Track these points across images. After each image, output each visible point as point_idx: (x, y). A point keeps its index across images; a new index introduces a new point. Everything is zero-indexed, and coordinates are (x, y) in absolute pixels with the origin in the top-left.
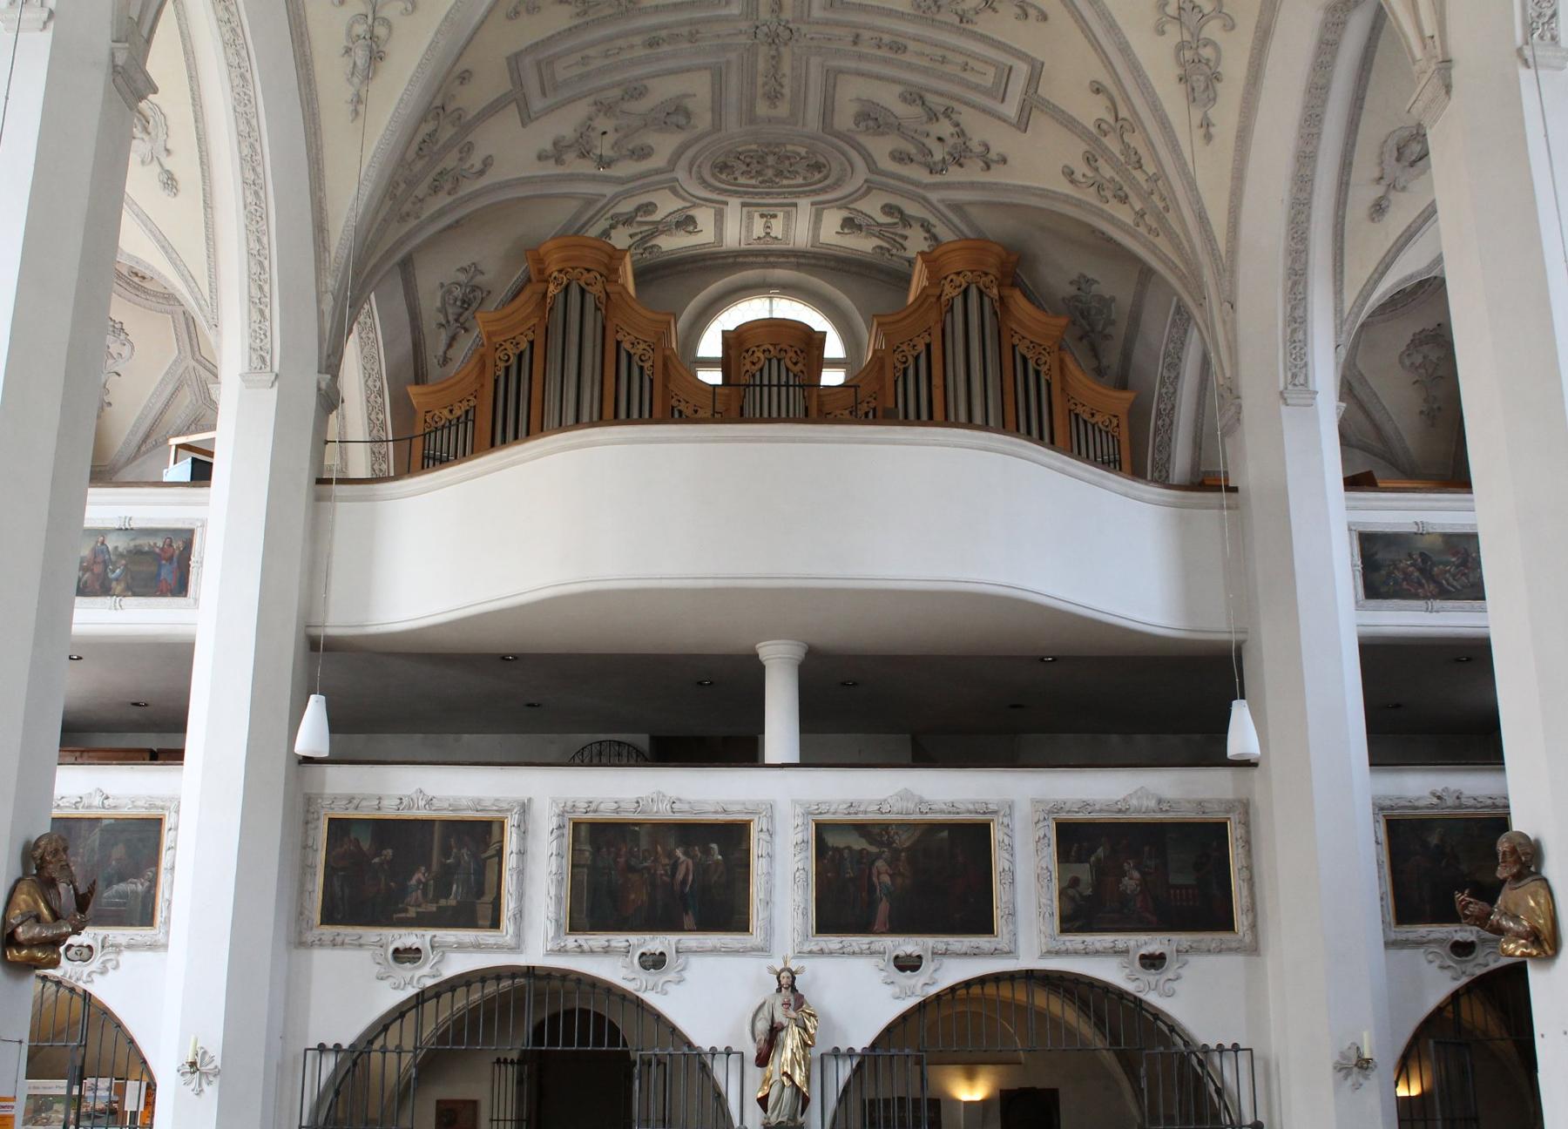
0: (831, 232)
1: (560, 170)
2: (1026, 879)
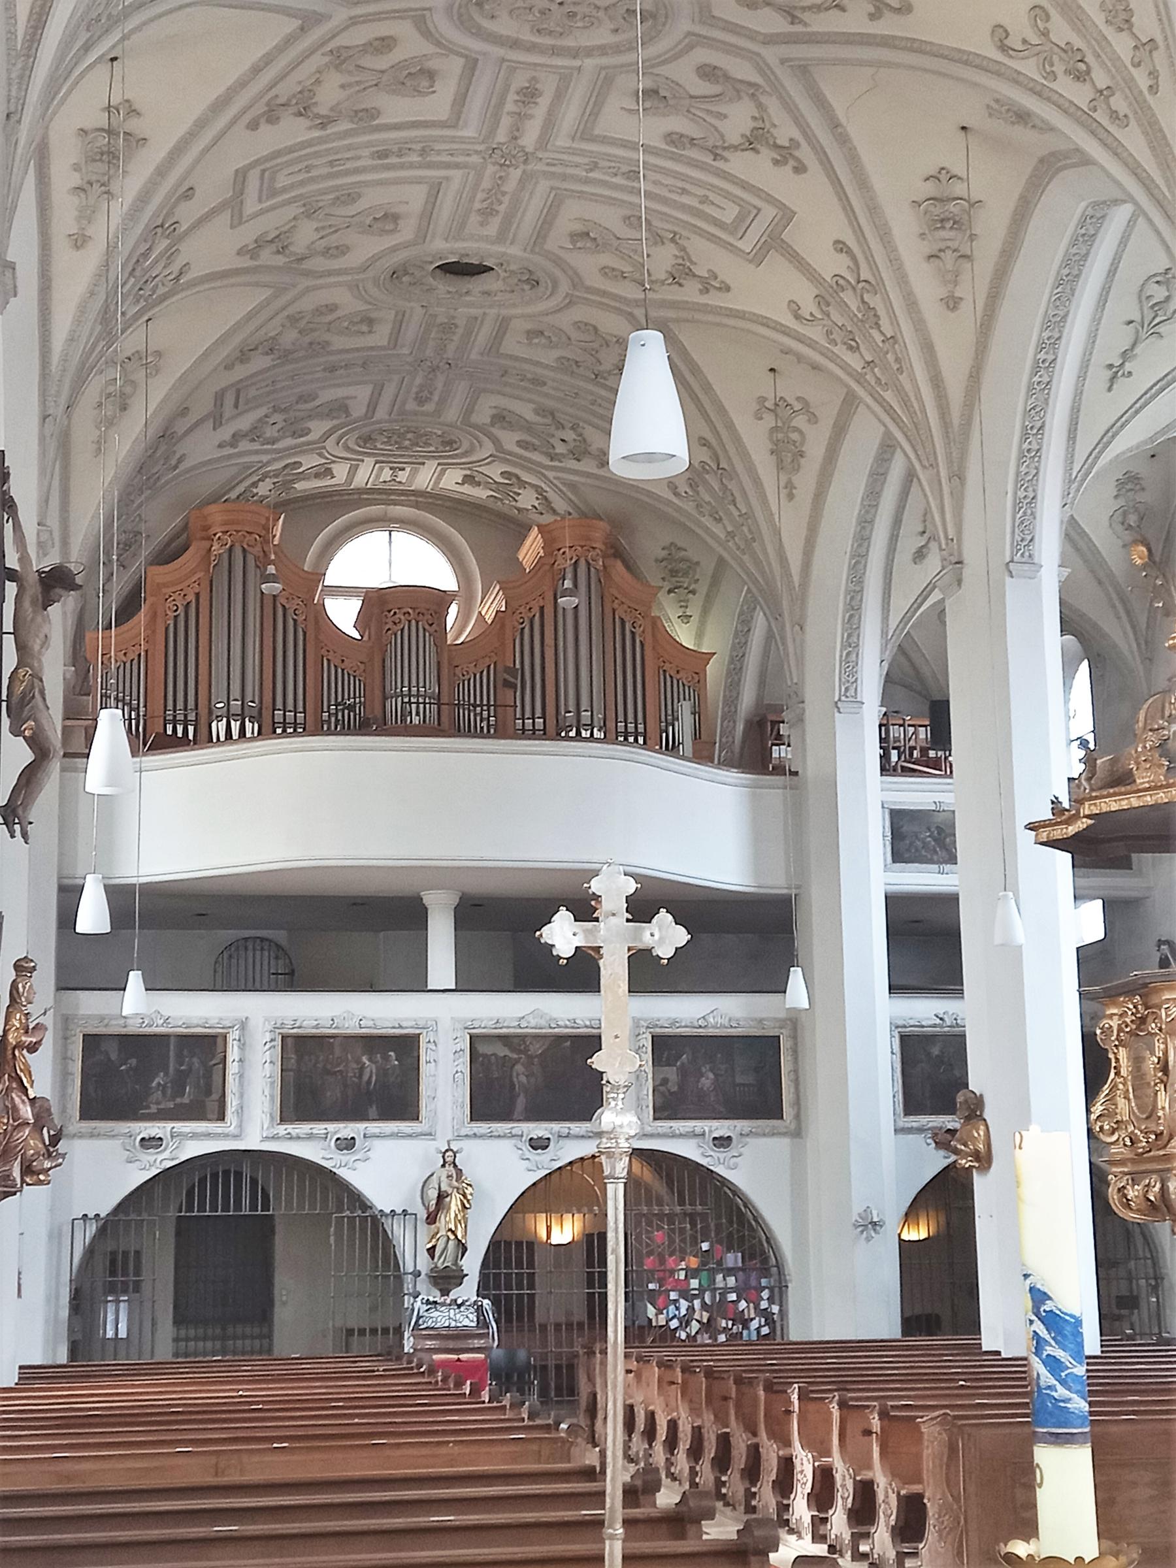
0: (452, 480)
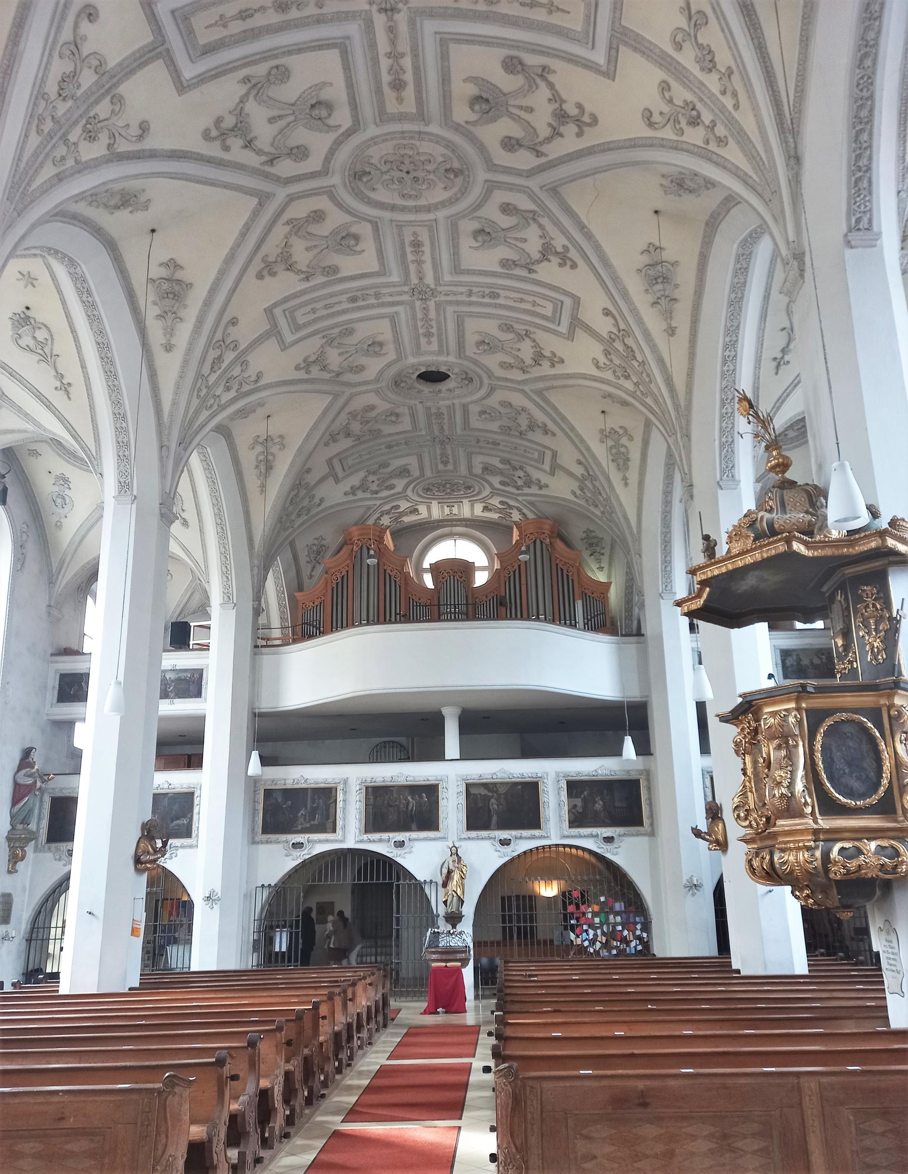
0: (478, 510)
1: (355, 498)
2: (554, 805)
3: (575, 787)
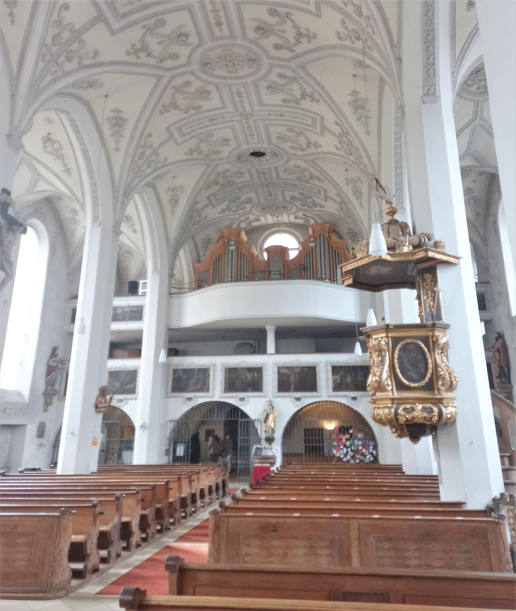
0: (292, 218)
2: (325, 379)
3: (336, 369)
